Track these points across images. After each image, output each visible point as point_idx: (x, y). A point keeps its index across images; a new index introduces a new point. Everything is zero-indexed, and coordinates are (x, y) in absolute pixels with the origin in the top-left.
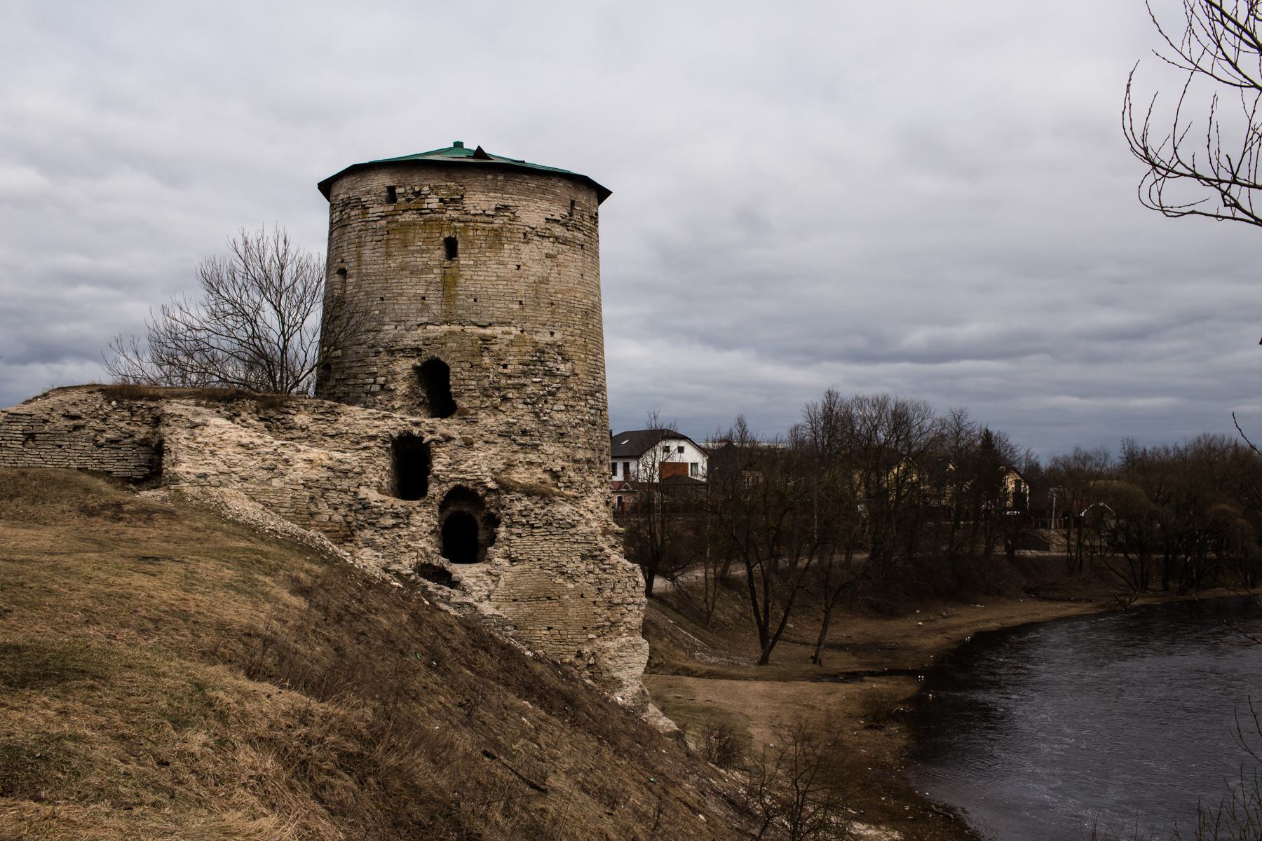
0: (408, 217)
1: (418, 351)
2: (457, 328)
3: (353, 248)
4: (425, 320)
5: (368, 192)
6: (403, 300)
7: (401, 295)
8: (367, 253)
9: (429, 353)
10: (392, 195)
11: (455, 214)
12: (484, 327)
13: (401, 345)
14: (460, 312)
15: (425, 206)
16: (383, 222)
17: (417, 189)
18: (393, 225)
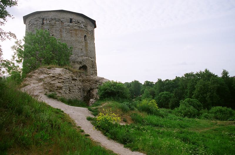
0: (76, 28)
1: (81, 63)
2: (88, 58)
3: (58, 32)
4: (83, 55)
5: (64, 18)
6: (77, 49)
7: (76, 48)
8: (64, 35)
9: (84, 64)
10: (71, 21)
11: (85, 30)
12: (91, 58)
13: (77, 61)
14: (89, 54)
15: (81, 26)
16: (69, 27)
17: (79, 21)
18: (73, 29)
